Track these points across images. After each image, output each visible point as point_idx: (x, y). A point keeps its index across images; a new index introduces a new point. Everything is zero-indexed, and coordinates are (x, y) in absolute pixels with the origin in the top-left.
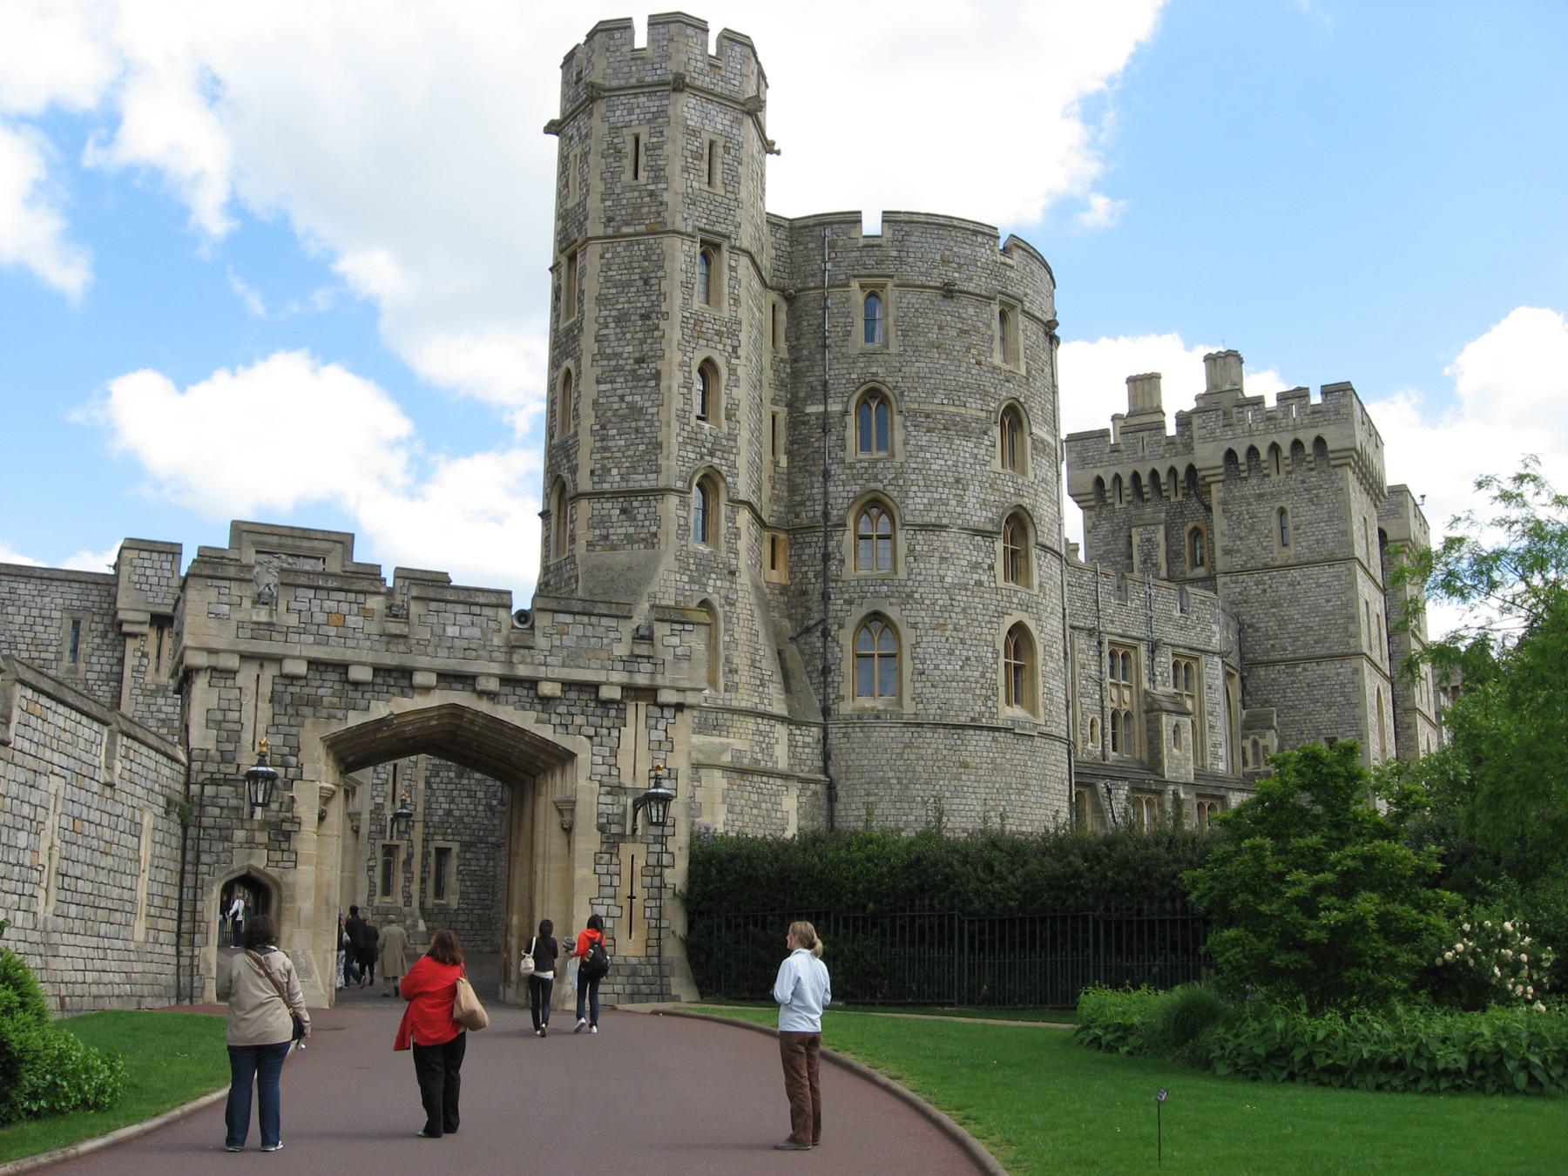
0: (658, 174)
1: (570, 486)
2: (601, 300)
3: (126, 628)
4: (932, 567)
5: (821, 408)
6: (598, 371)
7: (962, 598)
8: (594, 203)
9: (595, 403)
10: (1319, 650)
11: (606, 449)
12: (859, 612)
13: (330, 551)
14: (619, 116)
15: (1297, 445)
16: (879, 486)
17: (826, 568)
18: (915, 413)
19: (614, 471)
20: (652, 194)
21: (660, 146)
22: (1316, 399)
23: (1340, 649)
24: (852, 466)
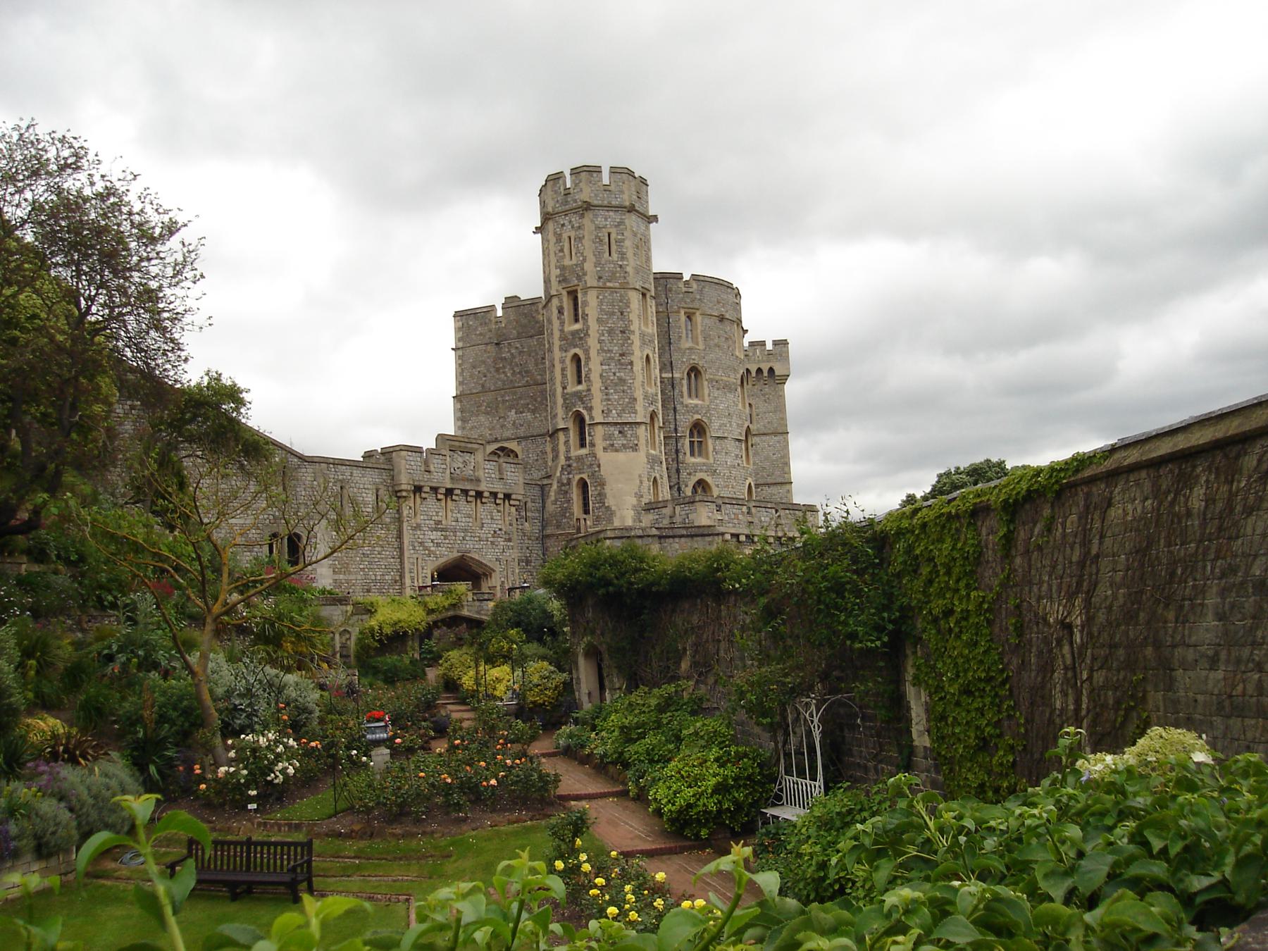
0: (623, 256)
1: (587, 418)
2: (599, 321)
3: (404, 494)
4: (722, 457)
6: (601, 359)
8: (588, 266)
9: (601, 376)
10: (769, 480)
11: (609, 400)
12: (694, 479)
13: (477, 450)
14: (600, 221)
15: (759, 371)
18: (710, 381)
20: (621, 266)
21: (623, 241)
22: (769, 346)
23: (780, 480)
24: (687, 406)
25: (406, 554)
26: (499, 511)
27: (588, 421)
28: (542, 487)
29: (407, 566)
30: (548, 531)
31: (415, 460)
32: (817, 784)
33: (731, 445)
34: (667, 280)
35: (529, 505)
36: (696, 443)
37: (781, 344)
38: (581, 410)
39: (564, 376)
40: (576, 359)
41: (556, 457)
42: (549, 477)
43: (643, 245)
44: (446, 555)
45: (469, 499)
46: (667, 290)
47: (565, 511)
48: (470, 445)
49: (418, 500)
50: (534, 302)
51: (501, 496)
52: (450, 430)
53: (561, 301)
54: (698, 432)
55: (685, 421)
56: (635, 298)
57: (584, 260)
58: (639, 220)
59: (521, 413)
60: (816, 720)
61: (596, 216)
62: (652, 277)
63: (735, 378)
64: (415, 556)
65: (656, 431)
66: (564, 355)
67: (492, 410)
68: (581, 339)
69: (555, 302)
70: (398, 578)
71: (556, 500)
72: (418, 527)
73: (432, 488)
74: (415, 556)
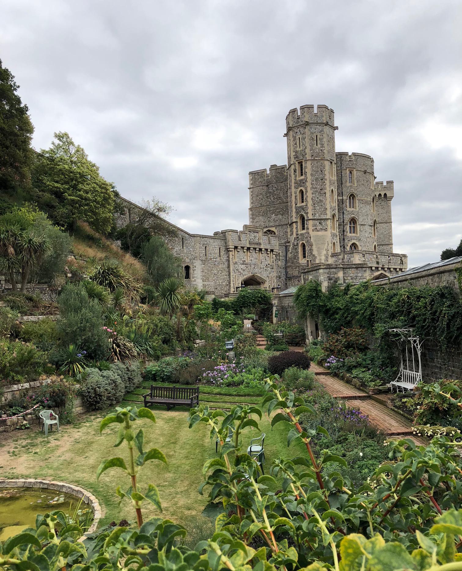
0: (322, 145)
2: (312, 175)
3: (230, 250)
4: (363, 233)
5: (342, 198)
7: (368, 240)
8: (307, 151)
9: (312, 199)
10: (382, 243)
11: (315, 209)
12: (351, 243)
14: (313, 130)
15: (380, 195)
16: (354, 216)
17: (344, 233)
18: (359, 200)
19: (317, 214)
20: (321, 150)
22: (385, 184)
23: (388, 243)
25: (231, 274)
26: (268, 257)
27: (306, 219)
28: (286, 246)
29: (232, 279)
30: (289, 264)
31: (235, 236)
32: (419, 374)
33: (367, 228)
34: (341, 156)
35: (281, 254)
36: (352, 228)
37: (390, 183)
38: (303, 214)
39: (296, 199)
40: (302, 192)
41: (292, 234)
42: (289, 242)
43: (331, 140)
44: (247, 275)
45: (256, 252)
46: (341, 160)
47: (296, 257)
48: (256, 229)
49: (236, 252)
50: (283, 167)
51: (269, 250)
52: (248, 223)
53: (295, 166)
54: (353, 222)
55: (347, 218)
56: (327, 164)
57: (306, 148)
58: (330, 129)
59: (277, 215)
60: (419, 347)
61: (311, 128)
62: (335, 154)
63: (370, 199)
64: (235, 275)
65: (335, 222)
66: (296, 190)
67: (265, 214)
68: (304, 183)
69: (293, 167)
70: (228, 284)
71: (292, 252)
72: (236, 263)
73: (241, 247)
74: (235, 275)
